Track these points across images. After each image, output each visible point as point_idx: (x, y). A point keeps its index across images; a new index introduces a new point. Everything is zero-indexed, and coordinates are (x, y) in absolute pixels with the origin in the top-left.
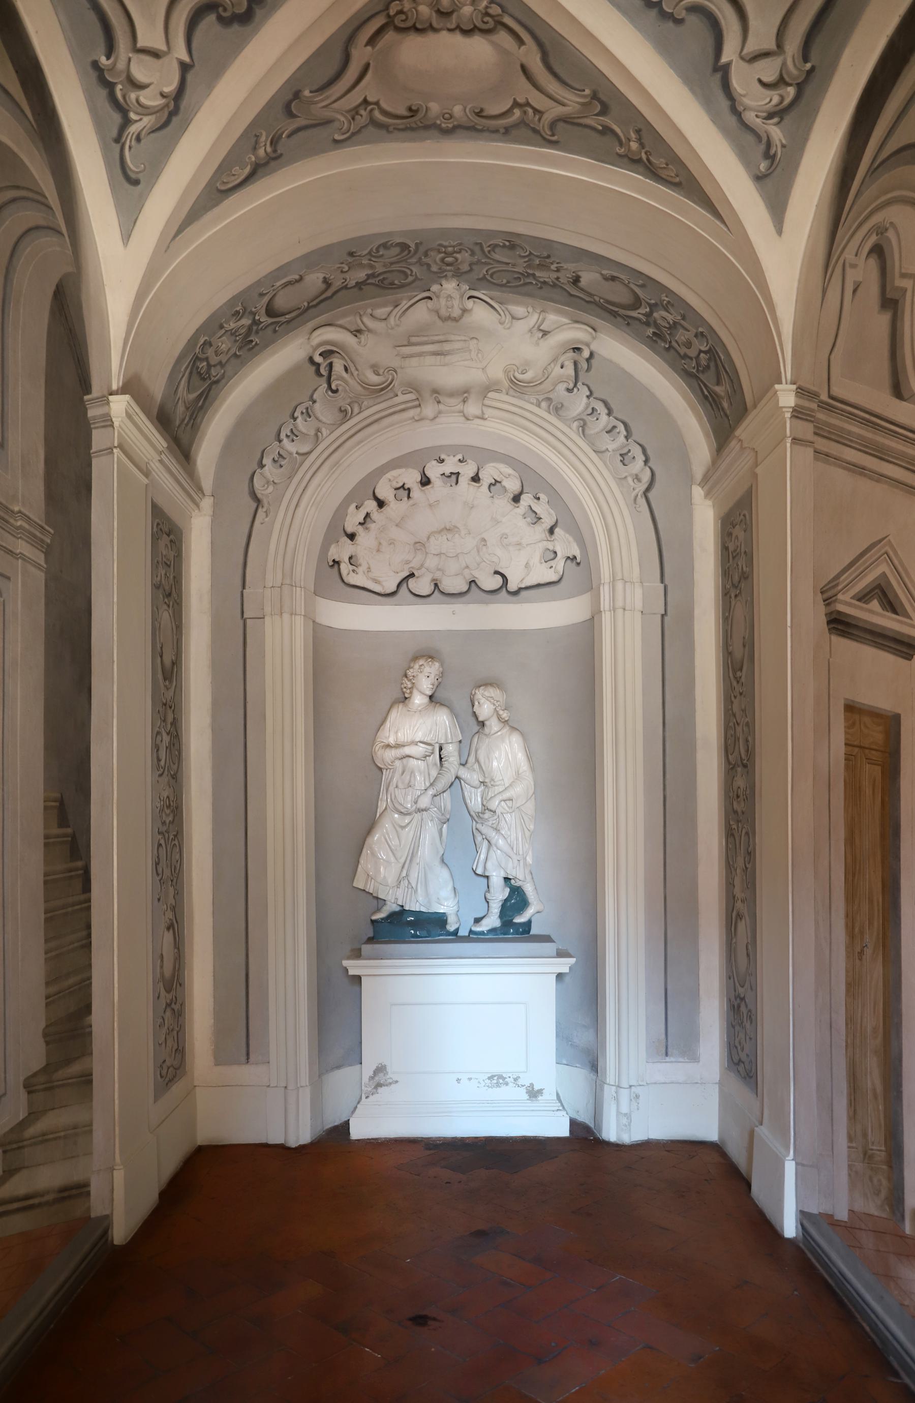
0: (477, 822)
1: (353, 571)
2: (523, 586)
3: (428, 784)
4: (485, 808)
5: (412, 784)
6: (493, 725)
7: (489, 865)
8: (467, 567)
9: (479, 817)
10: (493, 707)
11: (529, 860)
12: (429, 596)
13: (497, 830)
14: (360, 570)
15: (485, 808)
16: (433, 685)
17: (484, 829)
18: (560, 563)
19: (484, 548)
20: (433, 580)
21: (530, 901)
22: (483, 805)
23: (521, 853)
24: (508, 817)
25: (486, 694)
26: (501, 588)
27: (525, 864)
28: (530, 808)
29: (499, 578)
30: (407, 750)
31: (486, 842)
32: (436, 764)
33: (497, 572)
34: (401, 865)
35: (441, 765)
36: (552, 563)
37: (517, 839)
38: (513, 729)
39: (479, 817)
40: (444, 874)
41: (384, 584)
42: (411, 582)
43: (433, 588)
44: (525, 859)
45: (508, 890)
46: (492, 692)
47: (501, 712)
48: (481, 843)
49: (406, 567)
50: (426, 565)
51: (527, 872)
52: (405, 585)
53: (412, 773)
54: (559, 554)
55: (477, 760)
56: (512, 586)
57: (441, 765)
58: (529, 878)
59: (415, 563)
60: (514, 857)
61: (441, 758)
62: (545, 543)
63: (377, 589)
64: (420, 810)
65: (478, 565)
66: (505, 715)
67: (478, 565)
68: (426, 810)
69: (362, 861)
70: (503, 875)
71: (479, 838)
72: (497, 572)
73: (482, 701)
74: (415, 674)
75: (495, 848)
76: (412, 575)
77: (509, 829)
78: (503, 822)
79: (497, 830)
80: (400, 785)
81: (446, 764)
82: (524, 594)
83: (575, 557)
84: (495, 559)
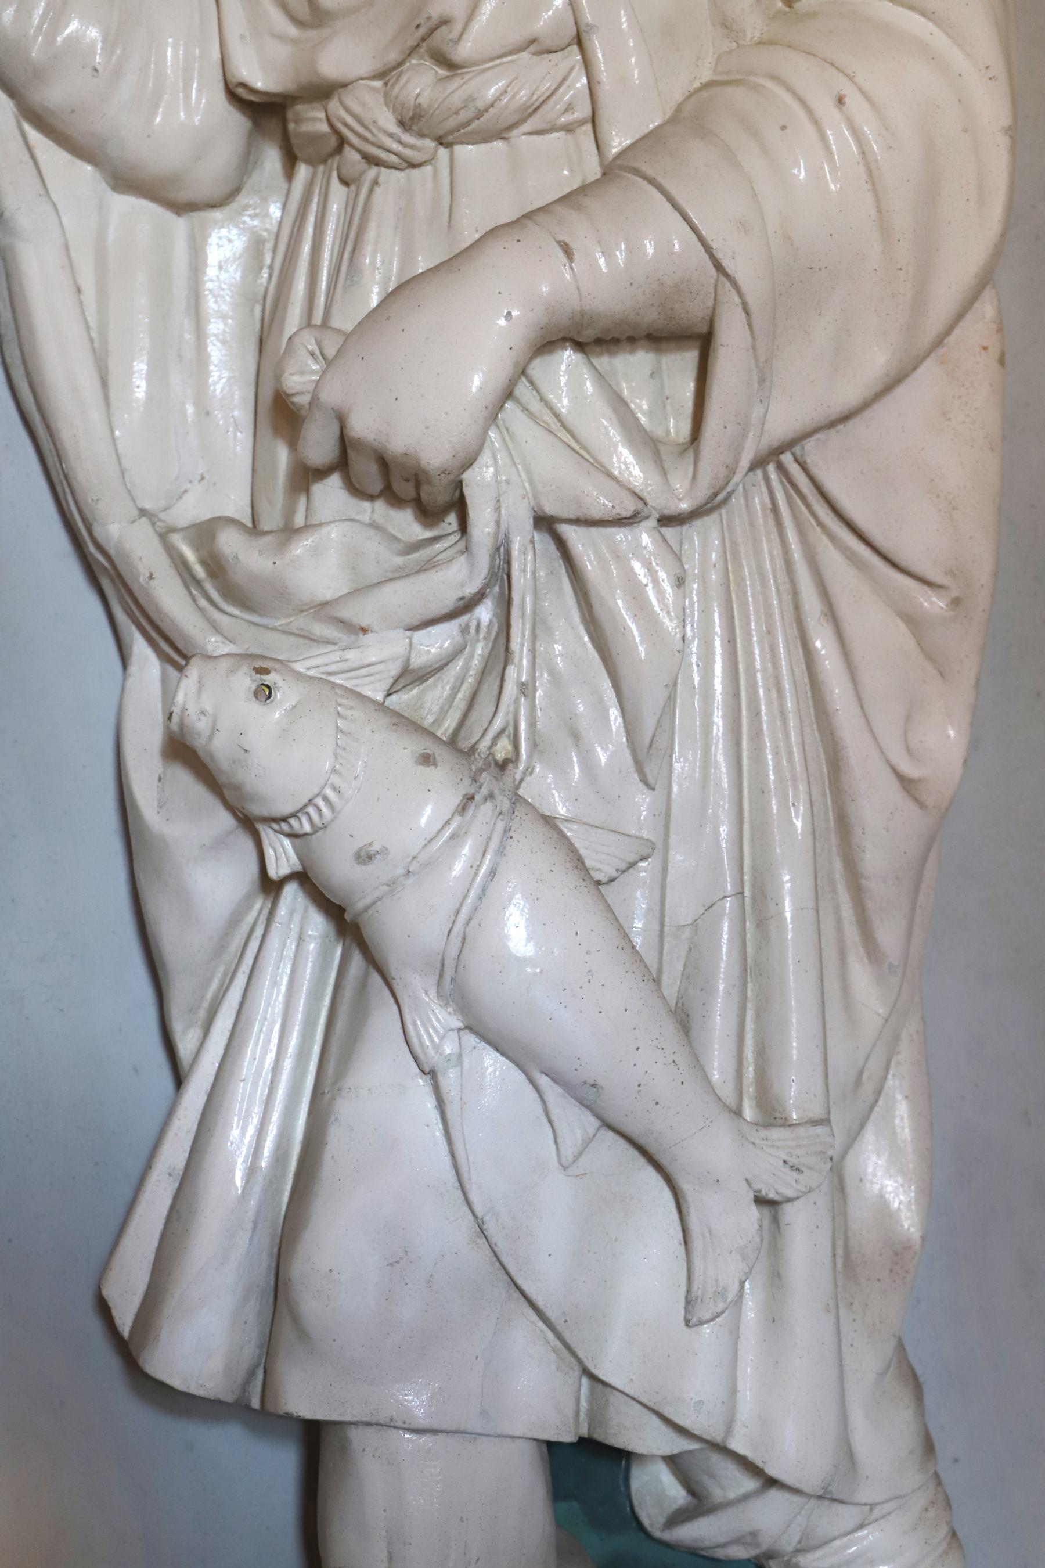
0: (176, 653)
4: (319, 449)
11: (889, 1183)
15: (319, 449)
17: (284, 748)
22: (281, 415)
23: (797, 1090)
24: (637, 570)
27: (847, 1263)
37: (757, 904)
39: (217, 578)
44: (839, 1183)
48: (239, 956)
51: (867, 1361)
58: (883, 1444)
60: (719, 1155)
70: (540, 1402)
71: (210, 880)
75: (437, 1025)
77: (646, 756)
78: (567, 643)
79: (483, 766)
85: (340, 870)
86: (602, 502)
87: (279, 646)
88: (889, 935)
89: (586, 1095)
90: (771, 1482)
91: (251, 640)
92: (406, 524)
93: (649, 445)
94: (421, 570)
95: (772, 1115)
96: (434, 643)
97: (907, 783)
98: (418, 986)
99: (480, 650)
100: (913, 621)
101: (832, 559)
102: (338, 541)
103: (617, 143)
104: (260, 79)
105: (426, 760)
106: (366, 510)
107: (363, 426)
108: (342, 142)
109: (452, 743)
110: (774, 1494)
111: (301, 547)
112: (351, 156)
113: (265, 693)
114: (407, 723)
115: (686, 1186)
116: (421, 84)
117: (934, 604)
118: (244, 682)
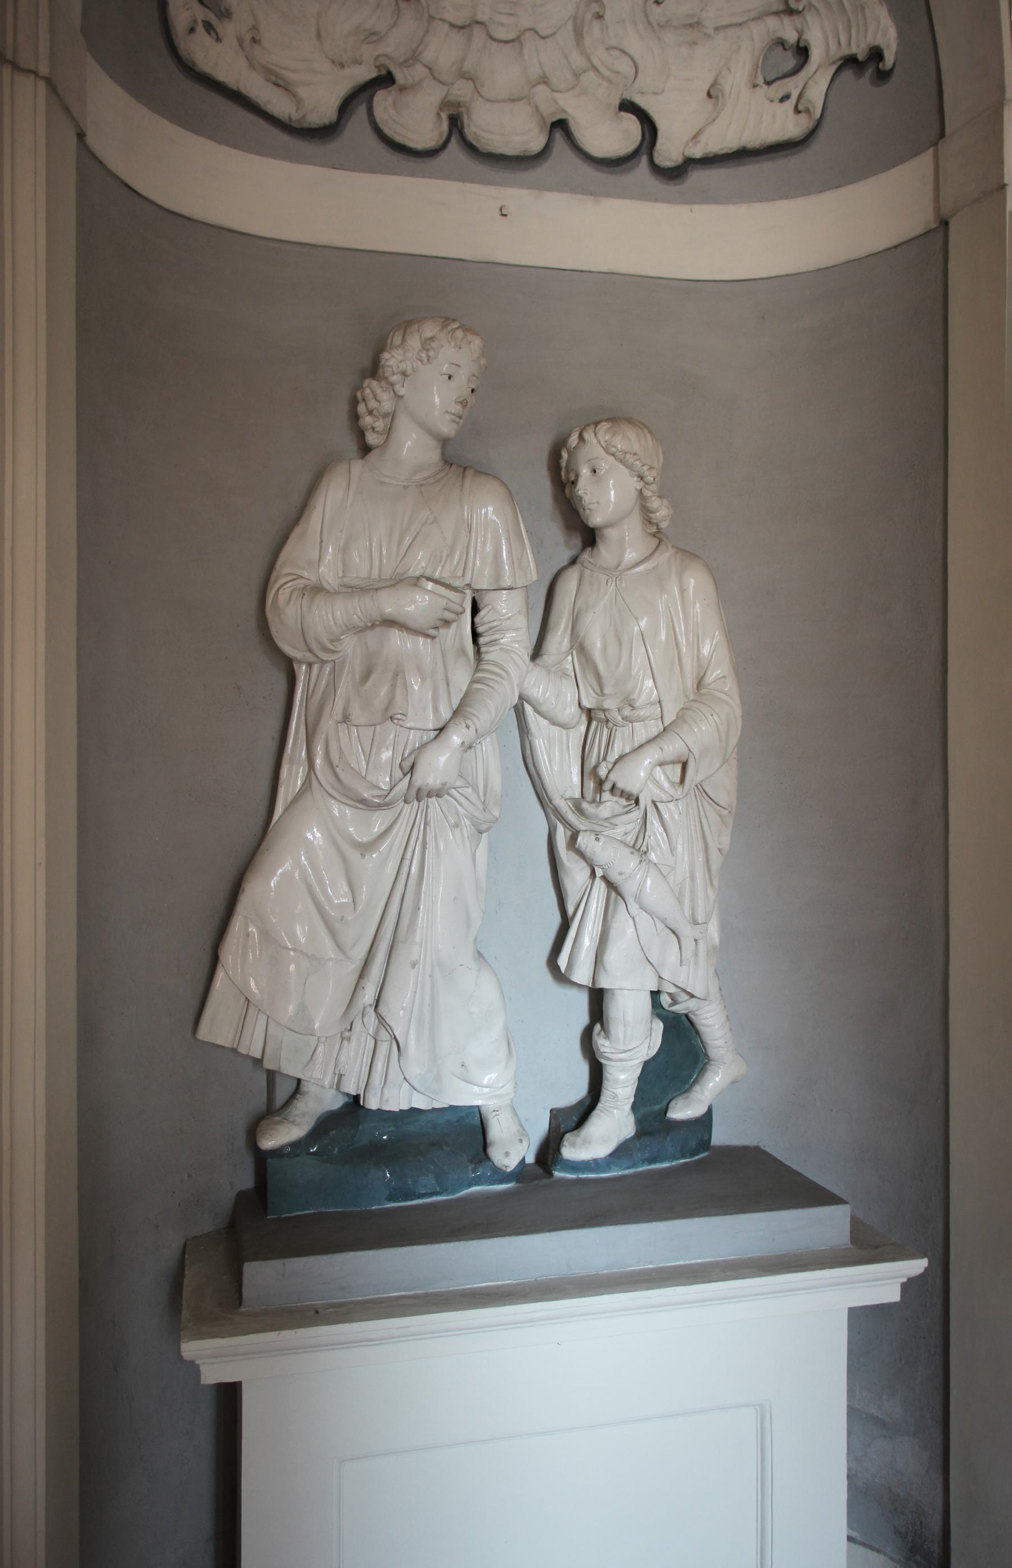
1: (208, 27)
2: (697, 152)
3: (446, 714)
5: (397, 709)
6: (625, 544)
7: (613, 956)
8: (544, 80)
9: (579, 810)
10: (635, 484)
12: (431, 153)
13: (639, 849)
14: (228, 30)
16: (464, 403)
18: (816, 83)
19: (596, 26)
20: (445, 104)
21: (712, 1053)
25: (620, 444)
26: (633, 156)
28: (724, 786)
29: (632, 125)
30: (389, 604)
31: (600, 887)
32: (463, 651)
33: (628, 106)
34: (353, 968)
35: (478, 652)
36: (793, 86)
38: (687, 554)
40: (486, 991)
41: (302, 92)
42: (383, 101)
43: (445, 126)
45: (659, 1026)
46: (628, 440)
47: (655, 503)
49: (369, 52)
50: (428, 56)
51: (711, 971)
52: (362, 109)
53: (398, 674)
54: (816, 55)
55: (580, 647)
56: (670, 149)
57: (478, 652)
59: (394, 46)
61: (475, 635)
62: (772, 23)
63: (279, 105)
64: (420, 795)
65: (577, 76)
66: (662, 511)
67: (577, 76)
68: (437, 794)
69: (228, 955)
72: (628, 106)
73: (606, 463)
74: (407, 366)
75: (634, 908)
76: (385, 80)
77: (672, 850)
80: (358, 715)
81: (491, 654)
82: (697, 177)
83: (876, 54)
84: (625, 66)
85: (614, 877)
86: (664, 797)
87: (599, 829)
88: (716, 883)
89: (663, 921)
90: (693, 996)
91: (590, 826)
92: (623, 802)
93: (672, 784)
94: (627, 813)
95: (695, 923)
96: (630, 827)
97: (720, 850)
98: (630, 900)
99: (638, 827)
100: (720, 816)
101: (705, 803)
102: (610, 805)
103: (666, 724)
104: (587, 704)
105: (632, 853)
106: (615, 799)
107: (620, 785)
108: (608, 721)
109: (633, 847)
110: (693, 999)
111: (601, 807)
112: (610, 725)
113: (597, 839)
114: (626, 845)
115: (682, 938)
116: (627, 712)
117: (726, 812)
118: (593, 837)
